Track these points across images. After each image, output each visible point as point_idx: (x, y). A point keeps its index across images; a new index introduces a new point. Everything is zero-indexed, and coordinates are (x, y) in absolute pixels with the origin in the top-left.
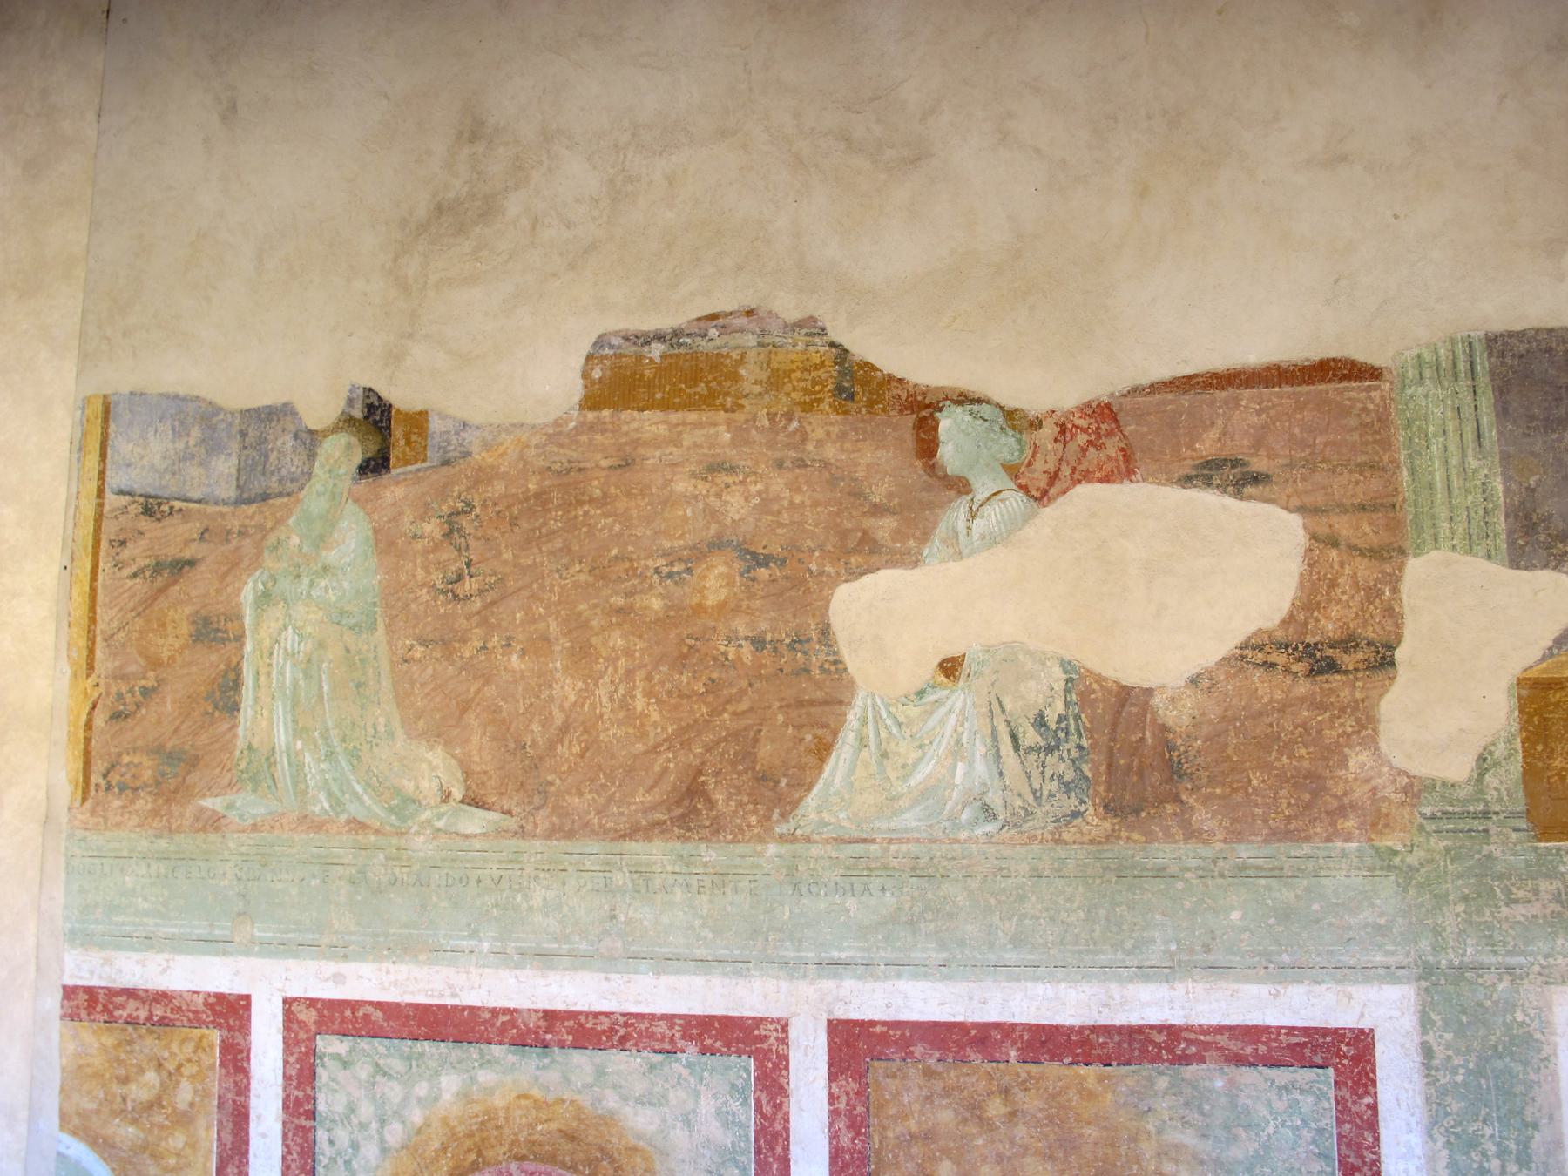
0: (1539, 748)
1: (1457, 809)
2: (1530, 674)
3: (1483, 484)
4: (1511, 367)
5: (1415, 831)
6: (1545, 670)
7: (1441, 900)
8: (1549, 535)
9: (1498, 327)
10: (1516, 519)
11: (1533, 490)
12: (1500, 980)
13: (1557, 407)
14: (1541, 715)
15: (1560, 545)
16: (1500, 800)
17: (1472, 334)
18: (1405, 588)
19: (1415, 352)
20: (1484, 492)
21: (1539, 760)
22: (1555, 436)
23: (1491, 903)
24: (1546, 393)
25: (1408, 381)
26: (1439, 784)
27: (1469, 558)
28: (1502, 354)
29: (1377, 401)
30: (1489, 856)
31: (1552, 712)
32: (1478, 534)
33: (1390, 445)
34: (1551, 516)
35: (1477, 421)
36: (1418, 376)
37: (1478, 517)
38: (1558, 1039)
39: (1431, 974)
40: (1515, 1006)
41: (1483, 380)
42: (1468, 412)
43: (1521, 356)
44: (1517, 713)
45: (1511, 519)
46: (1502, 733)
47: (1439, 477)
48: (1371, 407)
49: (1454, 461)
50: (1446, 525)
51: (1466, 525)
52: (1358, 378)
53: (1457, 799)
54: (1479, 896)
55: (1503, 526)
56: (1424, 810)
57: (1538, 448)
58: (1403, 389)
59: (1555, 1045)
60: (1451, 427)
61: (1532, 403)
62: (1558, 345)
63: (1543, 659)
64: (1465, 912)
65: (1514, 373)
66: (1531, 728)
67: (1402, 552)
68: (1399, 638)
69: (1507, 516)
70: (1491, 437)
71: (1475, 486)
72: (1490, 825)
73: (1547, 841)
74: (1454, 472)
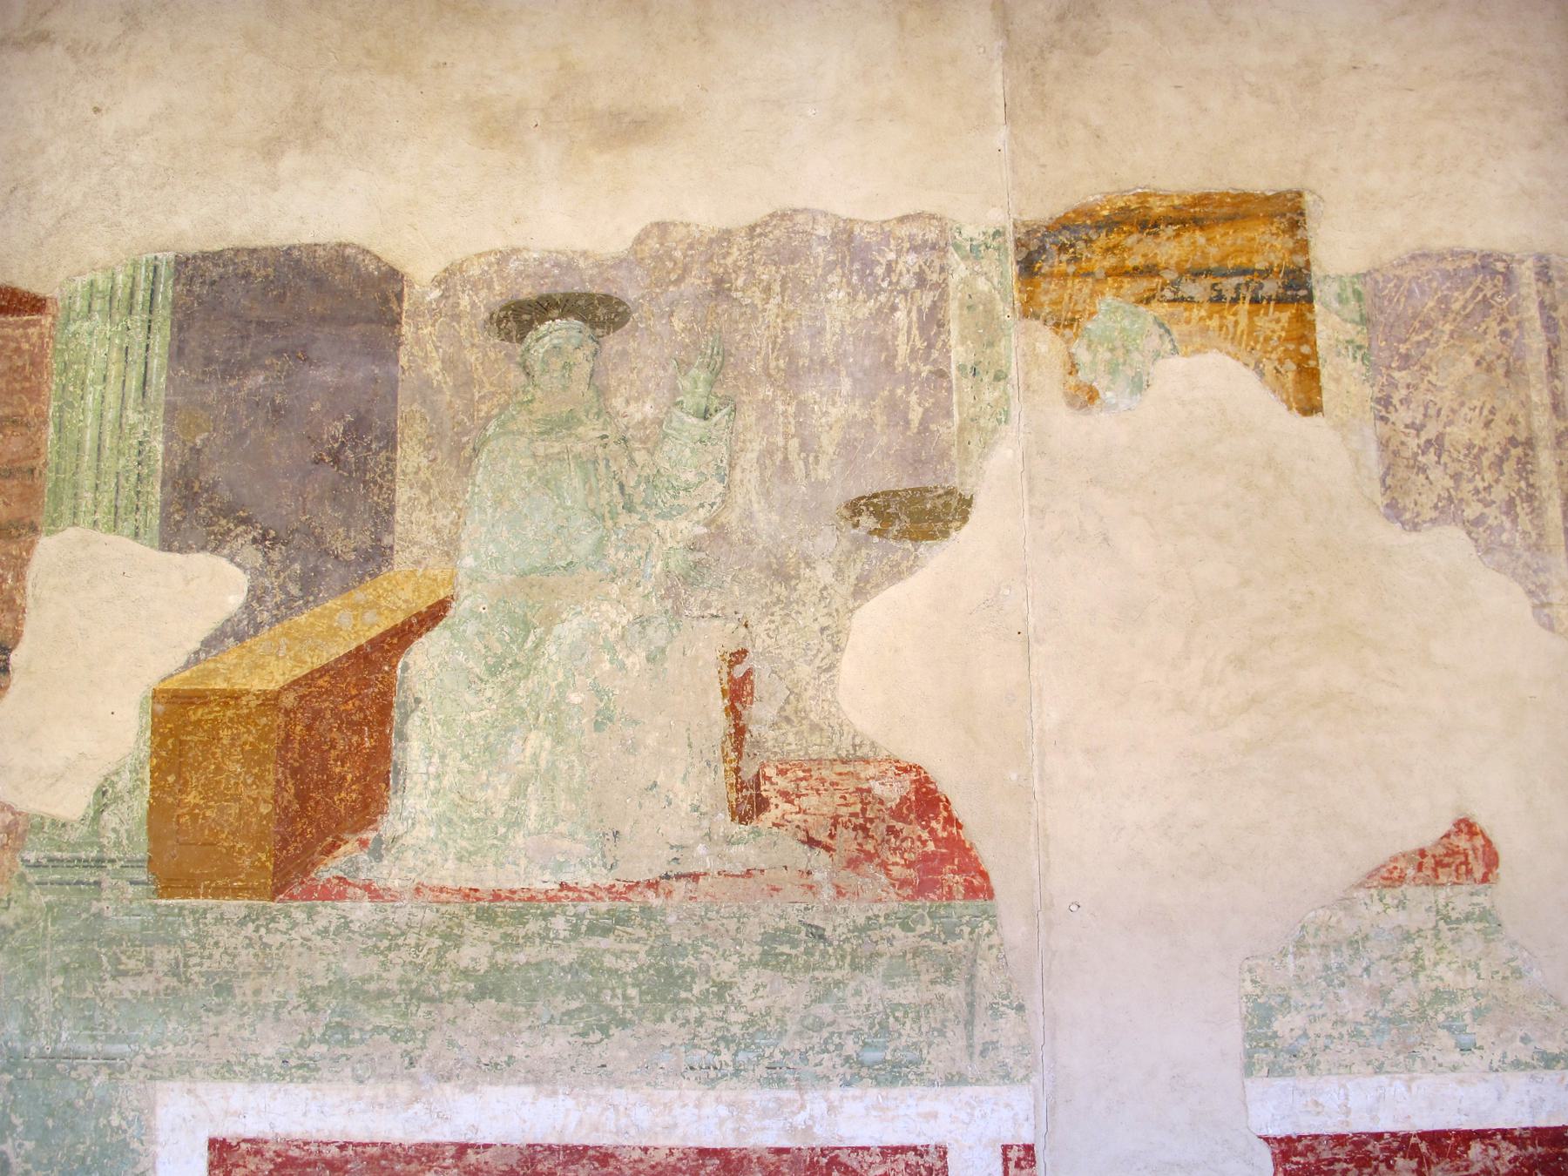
0: (171, 779)
1: (66, 855)
2: (172, 685)
3: (141, 443)
4: (199, 296)
5: (14, 882)
6: (186, 680)
7: (37, 969)
8: (212, 508)
9: (191, 247)
10: (174, 489)
11: (199, 452)
12: (97, 1073)
13: (242, 346)
14: (177, 737)
15: (223, 522)
16: (118, 844)
17: (160, 255)
18: (32, 572)
19: (88, 278)
20: (140, 453)
21: (169, 794)
22: (233, 383)
23: (94, 974)
24: (233, 328)
25: (73, 315)
26: (48, 822)
27: (112, 537)
28: (191, 279)
29: (35, 339)
30: (98, 916)
31: (190, 733)
32: (126, 507)
33: (39, 395)
34: (216, 484)
35: (146, 363)
36: (86, 309)
37: (128, 487)
38: (158, 1149)
39: (16, 1065)
40: (110, 1107)
41: (163, 313)
42: (137, 353)
43: (213, 283)
44: (148, 734)
45: (169, 488)
46: (128, 760)
47: (89, 436)
48: (26, 346)
49: (110, 415)
50: (89, 495)
51: (114, 493)
52: (17, 311)
53: (68, 843)
54: (82, 966)
55: (158, 496)
56: (27, 857)
57: (212, 397)
58: (66, 324)
59: (155, 1156)
60: (114, 371)
61: (214, 341)
62: (258, 270)
63: (187, 666)
64: (63, 986)
65: (199, 304)
66: (164, 754)
67: (34, 529)
68: (17, 636)
69: (164, 484)
70: (158, 384)
71: (131, 446)
72: (104, 875)
73: (170, 897)
74: (108, 428)
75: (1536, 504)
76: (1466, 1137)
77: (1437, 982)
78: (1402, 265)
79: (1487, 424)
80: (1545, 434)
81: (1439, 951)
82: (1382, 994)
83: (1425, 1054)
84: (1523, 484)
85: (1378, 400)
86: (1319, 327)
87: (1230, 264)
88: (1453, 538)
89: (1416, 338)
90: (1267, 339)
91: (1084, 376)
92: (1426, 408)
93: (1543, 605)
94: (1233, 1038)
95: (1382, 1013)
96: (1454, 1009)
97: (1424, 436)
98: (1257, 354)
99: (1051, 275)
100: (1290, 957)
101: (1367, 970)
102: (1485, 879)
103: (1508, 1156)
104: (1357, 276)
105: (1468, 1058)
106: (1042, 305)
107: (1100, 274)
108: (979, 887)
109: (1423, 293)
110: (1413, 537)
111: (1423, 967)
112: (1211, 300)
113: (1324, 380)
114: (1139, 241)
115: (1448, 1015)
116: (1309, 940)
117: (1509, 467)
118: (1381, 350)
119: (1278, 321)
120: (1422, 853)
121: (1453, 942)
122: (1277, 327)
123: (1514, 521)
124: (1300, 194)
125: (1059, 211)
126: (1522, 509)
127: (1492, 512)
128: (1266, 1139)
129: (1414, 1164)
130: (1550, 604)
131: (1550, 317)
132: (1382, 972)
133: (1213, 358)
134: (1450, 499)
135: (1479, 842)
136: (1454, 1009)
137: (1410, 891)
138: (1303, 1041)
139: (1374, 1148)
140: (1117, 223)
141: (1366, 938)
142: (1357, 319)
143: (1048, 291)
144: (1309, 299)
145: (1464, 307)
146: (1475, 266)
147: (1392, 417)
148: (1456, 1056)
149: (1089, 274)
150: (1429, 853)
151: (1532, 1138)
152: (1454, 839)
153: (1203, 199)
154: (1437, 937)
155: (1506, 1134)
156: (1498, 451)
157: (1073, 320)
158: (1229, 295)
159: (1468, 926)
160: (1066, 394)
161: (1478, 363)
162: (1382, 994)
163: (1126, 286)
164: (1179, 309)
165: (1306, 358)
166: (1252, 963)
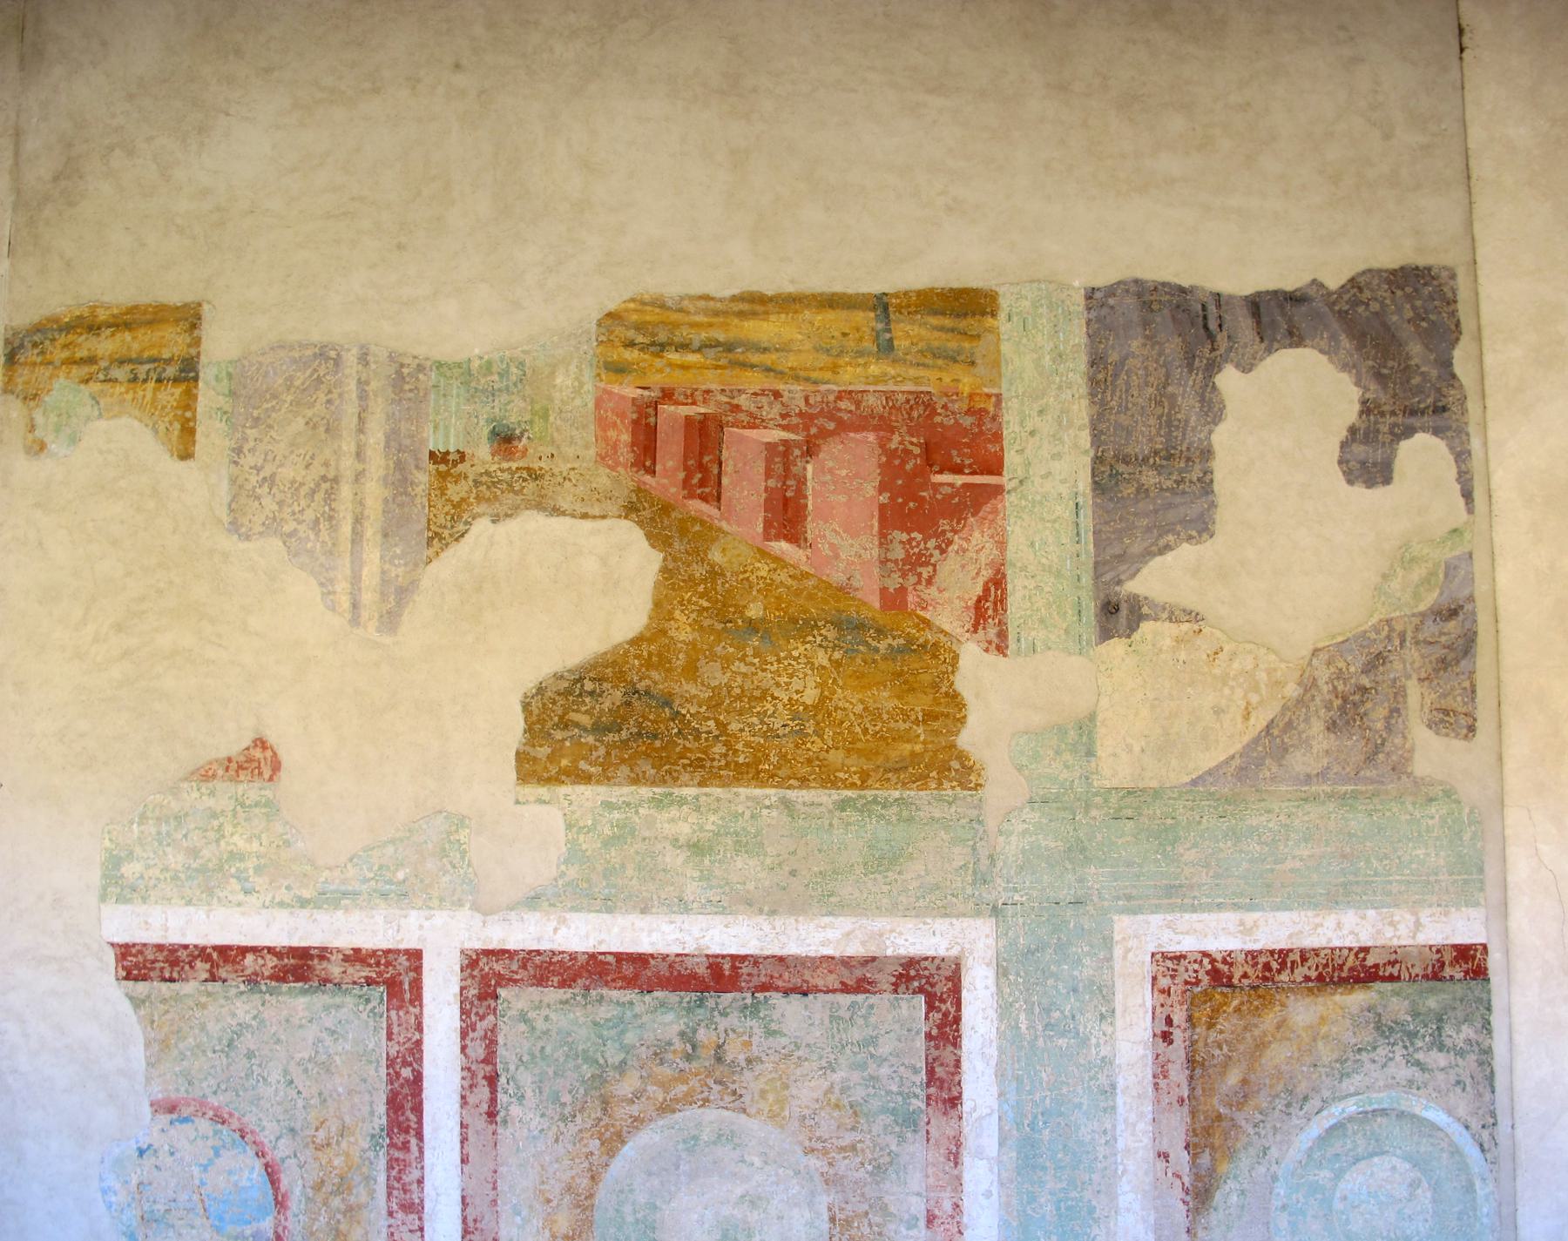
75: (334, 522)
76: (244, 950)
77: (232, 847)
78: (263, 354)
79: (307, 467)
80: (348, 472)
81: (235, 826)
82: (194, 852)
83: (221, 894)
84: (327, 508)
85: (233, 450)
86: (200, 398)
87: (146, 355)
88: (276, 543)
89: (266, 406)
90: (164, 407)
91: (38, 433)
92: (266, 455)
93: (329, 593)
94: (95, 877)
95: (194, 866)
96: (242, 866)
97: (262, 475)
98: (155, 418)
99: (26, 364)
100: (135, 825)
101: (185, 836)
102: (271, 779)
103: (270, 964)
104: (231, 362)
105: (249, 898)
106: (17, 385)
107: (58, 363)
109: (275, 373)
110: (243, 545)
111: (223, 836)
112: (129, 381)
113: (198, 436)
114: (87, 339)
115: (238, 869)
116: (149, 814)
117: (319, 496)
118: (240, 414)
119: (172, 395)
120: (230, 760)
121: (246, 820)
122: (172, 399)
123: (317, 535)
124: (200, 305)
125: (36, 319)
126: (323, 526)
127: (302, 528)
128: (112, 945)
129: (208, 966)
130: (335, 593)
131: (363, 390)
132: (195, 839)
133: (124, 420)
134: (274, 519)
135: (269, 754)
136: (242, 866)
137: (219, 785)
138: (140, 881)
139: (183, 954)
140: (73, 327)
141: (186, 815)
142: (227, 392)
143: (23, 375)
144: (196, 379)
145: (303, 384)
146: (315, 354)
147: (241, 462)
148: (241, 897)
149: (50, 363)
150: (234, 760)
151: (288, 954)
152: (252, 752)
153: (134, 309)
154: (235, 816)
155: (270, 950)
156: (312, 485)
157: (36, 395)
158: (142, 376)
159: (257, 810)
160: (25, 446)
161: (307, 423)
162: (194, 852)
163: (74, 371)
164: (107, 386)
165: (188, 420)
166: (111, 827)
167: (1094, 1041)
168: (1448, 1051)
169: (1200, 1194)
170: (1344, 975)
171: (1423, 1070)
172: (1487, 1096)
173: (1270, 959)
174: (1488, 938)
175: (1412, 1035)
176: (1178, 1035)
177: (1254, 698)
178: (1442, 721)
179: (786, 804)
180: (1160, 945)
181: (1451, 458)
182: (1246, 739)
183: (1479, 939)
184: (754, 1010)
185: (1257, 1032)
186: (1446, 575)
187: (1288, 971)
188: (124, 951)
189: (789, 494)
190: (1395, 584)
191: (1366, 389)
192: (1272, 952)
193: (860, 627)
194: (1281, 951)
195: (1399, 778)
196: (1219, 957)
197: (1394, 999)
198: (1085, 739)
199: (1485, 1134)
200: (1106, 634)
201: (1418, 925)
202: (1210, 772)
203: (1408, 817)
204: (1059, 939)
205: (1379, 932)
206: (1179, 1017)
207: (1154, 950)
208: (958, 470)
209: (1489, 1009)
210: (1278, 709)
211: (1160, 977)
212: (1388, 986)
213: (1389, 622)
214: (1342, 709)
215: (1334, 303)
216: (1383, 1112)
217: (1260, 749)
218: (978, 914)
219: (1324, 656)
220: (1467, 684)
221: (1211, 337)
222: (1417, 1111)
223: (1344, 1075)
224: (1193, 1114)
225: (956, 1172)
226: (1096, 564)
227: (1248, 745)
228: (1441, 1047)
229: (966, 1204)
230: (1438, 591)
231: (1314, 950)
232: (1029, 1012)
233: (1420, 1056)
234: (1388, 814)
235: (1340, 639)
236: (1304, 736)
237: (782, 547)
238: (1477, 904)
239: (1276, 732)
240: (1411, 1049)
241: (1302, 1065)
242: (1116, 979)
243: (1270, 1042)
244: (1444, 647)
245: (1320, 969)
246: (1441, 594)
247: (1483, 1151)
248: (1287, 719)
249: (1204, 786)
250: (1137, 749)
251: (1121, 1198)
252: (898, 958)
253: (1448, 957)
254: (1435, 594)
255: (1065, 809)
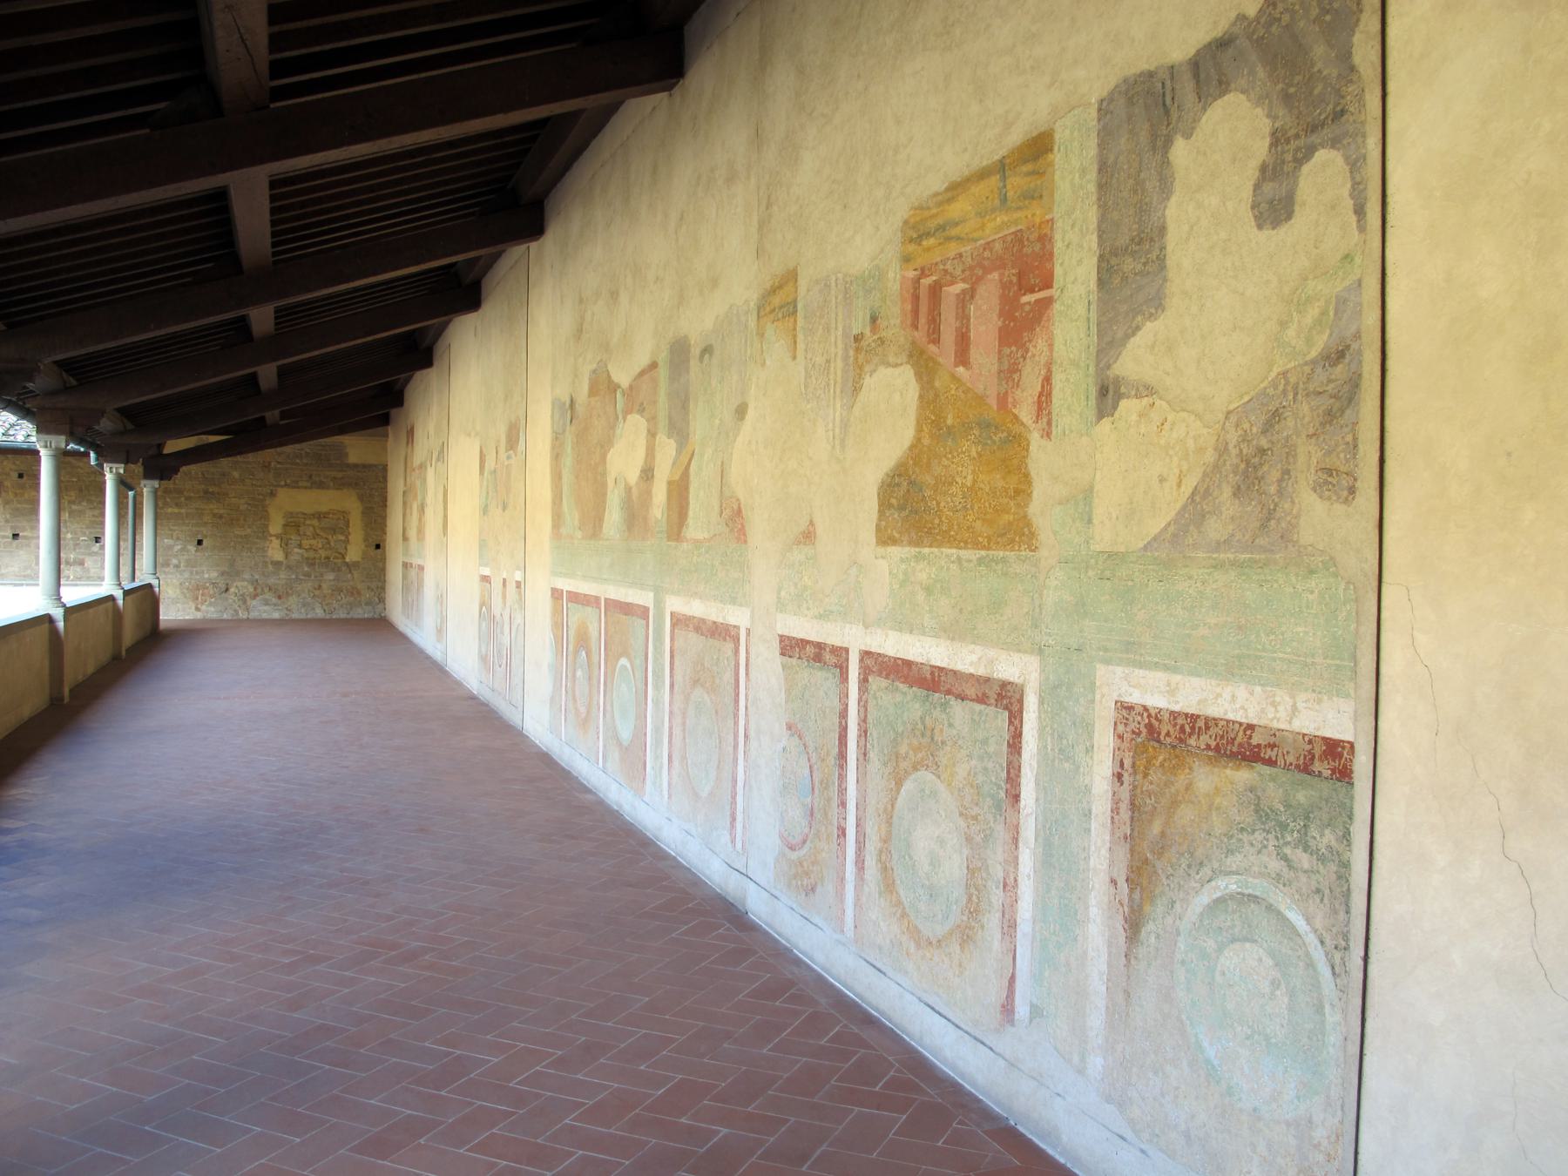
108: (745, 542)
167: (1082, 769)
168: (1311, 854)
169: (1134, 925)
170: (1235, 749)
171: (1290, 867)
172: (1342, 915)
173: (1185, 722)
174: (1355, 735)
175: (1283, 827)
176: (1126, 777)
177: (1185, 468)
178: (1326, 482)
179: (959, 559)
180: (1120, 695)
181: (1347, 168)
182: (1178, 506)
183: (1348, 737)
184: (944, 706)
185: (1173, 790)
186: (1336, 313)
187: (1196, 736)
188: (782, 638)
189: (964, 330)
190: (1291, 332)
191: (1274, 118)
192: (1186, 715)
193: (988, 426)
194: (1193, 715)
195: (1286, 547)
196: (1153, 713)
197: (1271, 784)
198: (1087, 509)
199: (1337, 956)
200: (1101, 414)
201: (1295, 709)
202: (1155, 539)
203: (1292, 590)
204: (1069, 679)
205: (1263, 710)
206: (1127, 763)
207: (1117, 699)
208: (1032, 291)
209: (1350, 817)
210: (1200, 475)
211: (1118, 723)
212: (1267, 770)
213: (1285, 374)
214: (1246, 475)
215: (1253, 33)
216: (1254, 898)
217: (1187, 515)
218: (1032, 653)
219: (1233, 418)
220: (1349, 438)
221: (1167, 112)
222: (1282, 908)
223: (1230, 852)
224: (1132, 851)
225: (1016, 854)
226: (1098, 351)
227: (1179, 513)
228: (1306, 848)
229: (1019, 879)
230: (1328, 331)
231: (1214, 719)
232: (1052, 734)
233: (1287, 850)
234: (1275, 585)
235: (1246, 399)
236: (1217, 501)
237: (961, 369)
238: (1347, 696)
239: (1197, 498)
240: (1281, 841)
241: (1200, 831)
242: (1096, 720)
243: (1180, 802)
244: (1331, 397)
245: (1218, 740)
246: (1331, 335)
247: (1334, 974)
248: (1205, 486)
249: (1151, 551)
250: (1114, 516)
251: (1091, 908)
252: (999, 680)
253: (1317, 752)
254: (1325, 337)
255: (1075, 569)
